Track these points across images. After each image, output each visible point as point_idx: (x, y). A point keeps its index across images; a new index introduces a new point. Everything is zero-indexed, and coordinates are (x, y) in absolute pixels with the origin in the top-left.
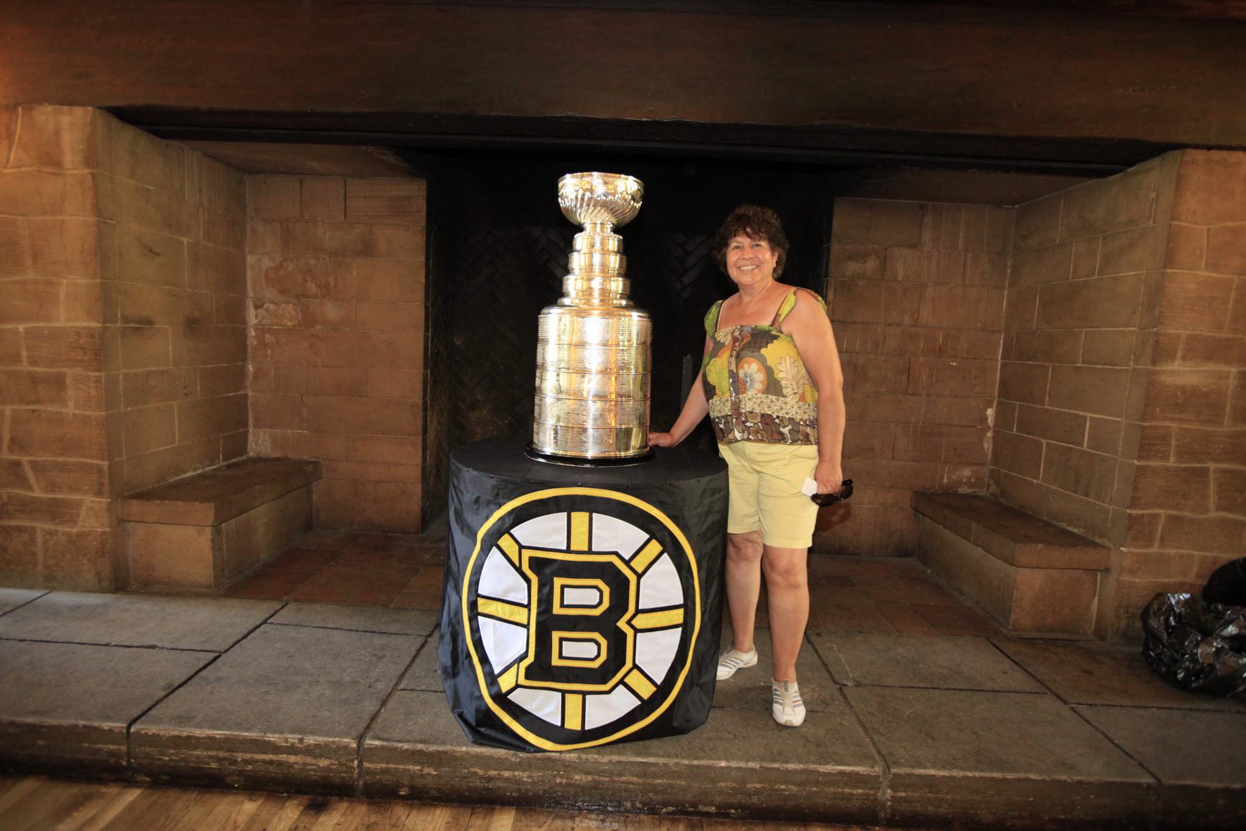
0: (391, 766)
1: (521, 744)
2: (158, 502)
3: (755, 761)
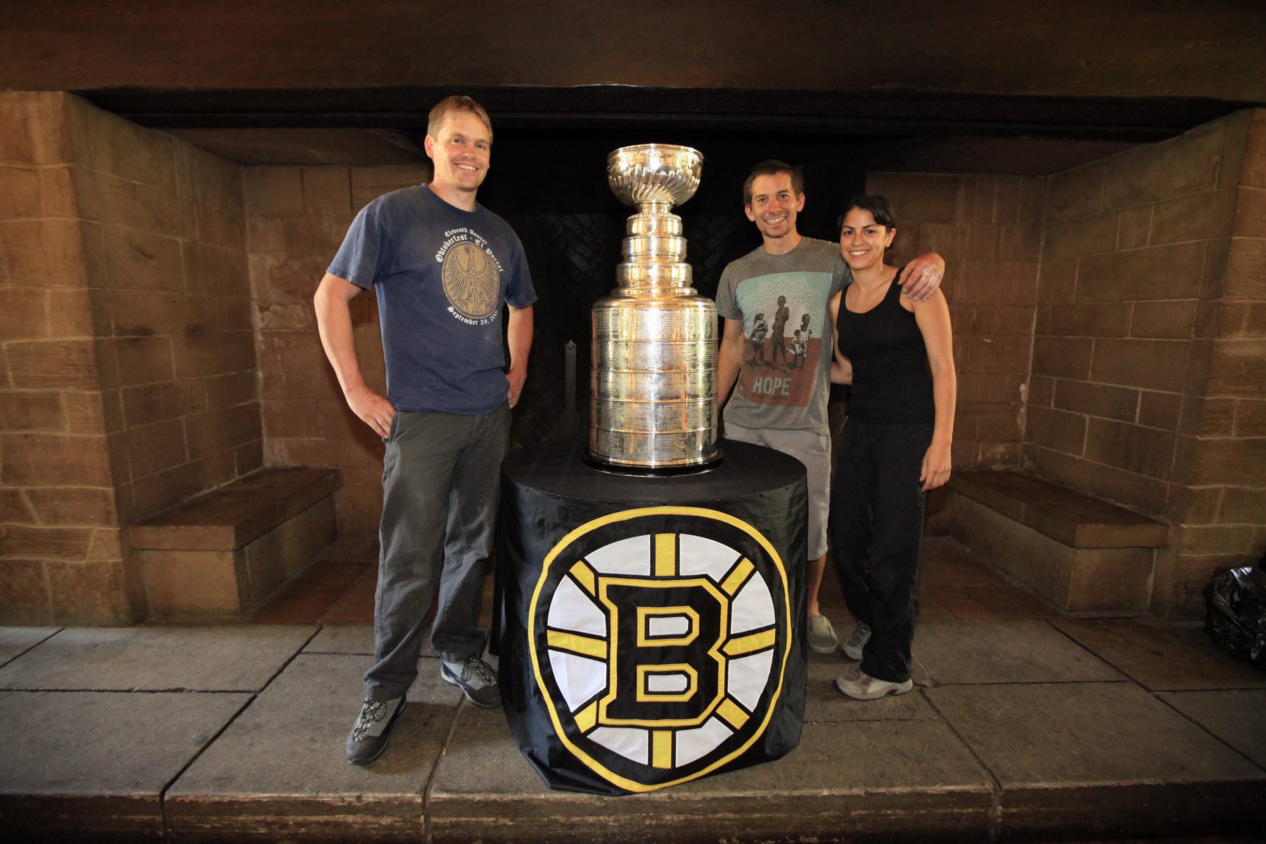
0: (462, 819)
1: (603, 787)
2: (173, 527)
3: (859, 786)
